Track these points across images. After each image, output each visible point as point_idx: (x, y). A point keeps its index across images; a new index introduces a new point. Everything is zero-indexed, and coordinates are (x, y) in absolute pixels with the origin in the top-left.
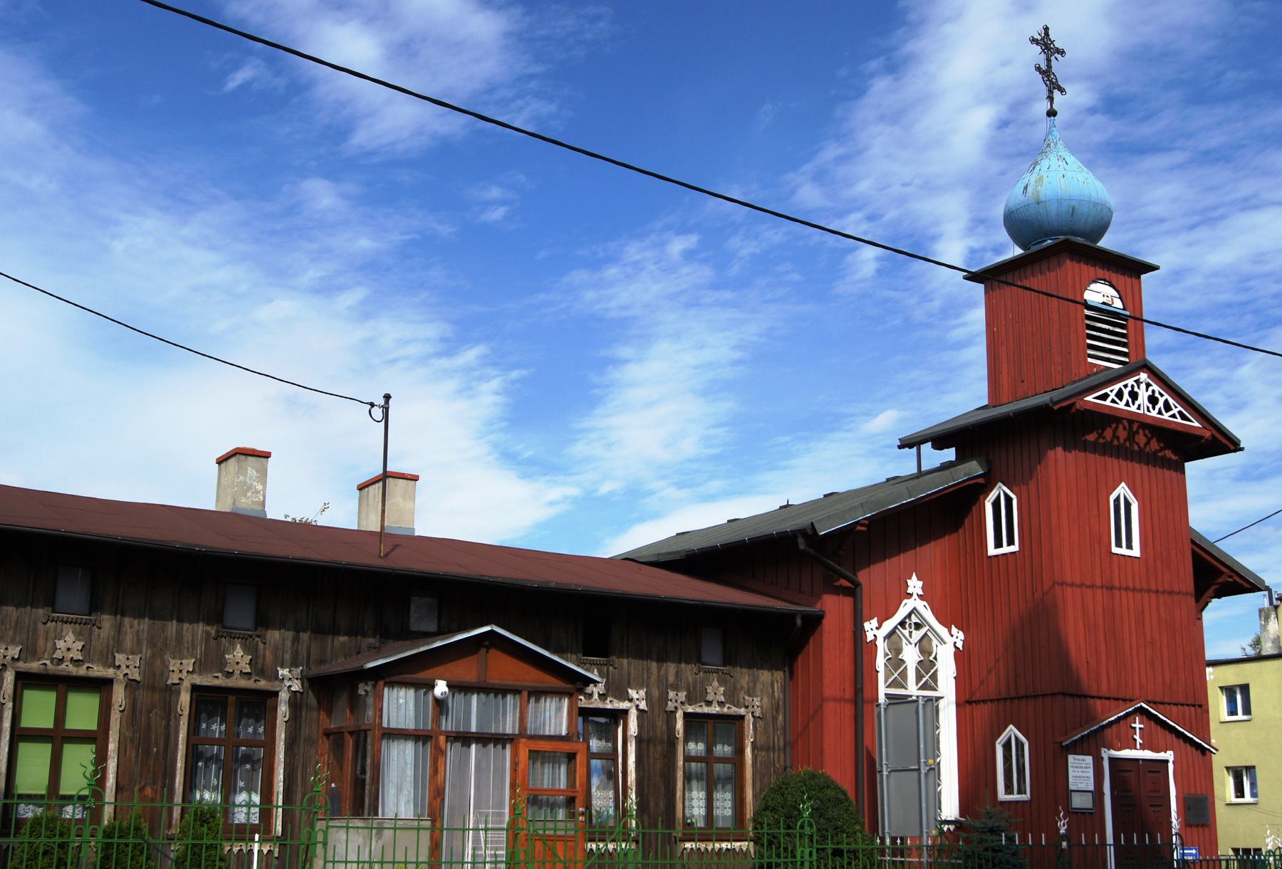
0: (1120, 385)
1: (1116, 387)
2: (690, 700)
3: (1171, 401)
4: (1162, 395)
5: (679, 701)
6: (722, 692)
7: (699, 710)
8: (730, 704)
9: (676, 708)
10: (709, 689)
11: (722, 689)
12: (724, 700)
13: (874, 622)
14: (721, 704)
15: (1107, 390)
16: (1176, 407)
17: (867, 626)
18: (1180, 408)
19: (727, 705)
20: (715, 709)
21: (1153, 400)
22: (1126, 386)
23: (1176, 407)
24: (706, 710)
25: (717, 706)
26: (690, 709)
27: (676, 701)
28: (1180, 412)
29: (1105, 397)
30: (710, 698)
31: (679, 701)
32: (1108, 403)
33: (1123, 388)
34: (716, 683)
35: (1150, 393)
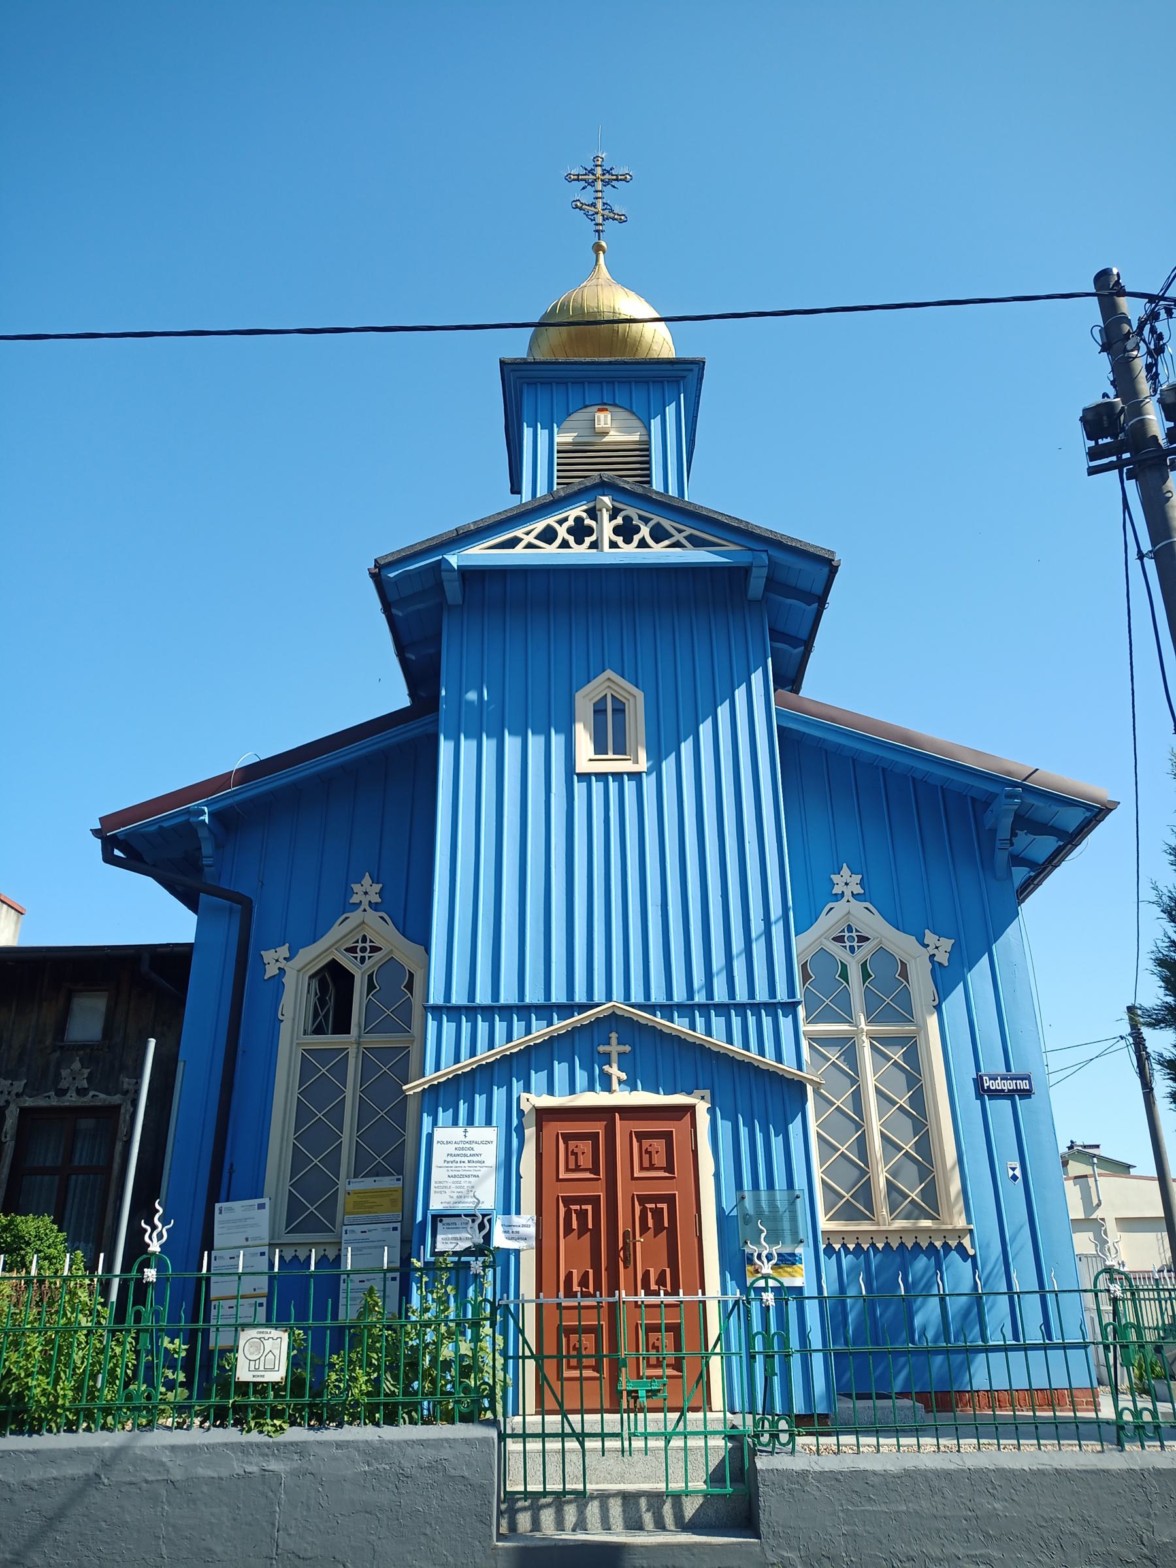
0: (551, 521)
1: (540, 526)
2: (33, 1089)
3: (667, 524)
4: (646, 521)
5: (14, 1093)
6: (86, 1076)
7: (41, 1102)
8: (96, 1090)
9: (8, 1102)
10: (65, 1073)
11: (86, 1072)
12: (86, 1086)
13: (284, 951)
14: (81, 1092)
15: (519, 533)
16: (680, 531)
17: (268, 956)
18: (689, 531)
19: (92, 1093)
20: (72, 1099)
21: (626, 531)
22: (561, 522)
23: (680, 531)
24: (54, 1102)
25: (74, 1094)
26: (29, 1102)
27: (9, 1093)
28: (688, 538)
29: (513, 543)
30: (64, 1084)
31: (14, 1093)
32: (519, 549)
33: (556, 526)
34: (77, 1065)
35: (619, 520)
